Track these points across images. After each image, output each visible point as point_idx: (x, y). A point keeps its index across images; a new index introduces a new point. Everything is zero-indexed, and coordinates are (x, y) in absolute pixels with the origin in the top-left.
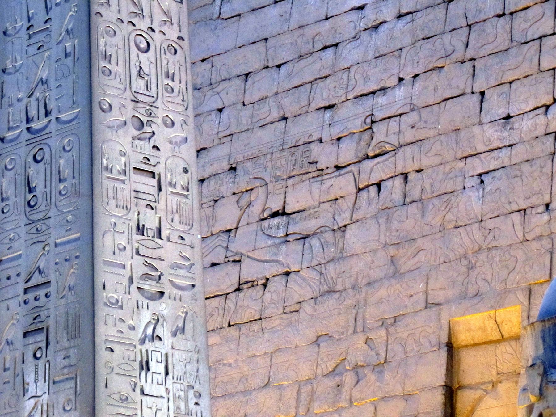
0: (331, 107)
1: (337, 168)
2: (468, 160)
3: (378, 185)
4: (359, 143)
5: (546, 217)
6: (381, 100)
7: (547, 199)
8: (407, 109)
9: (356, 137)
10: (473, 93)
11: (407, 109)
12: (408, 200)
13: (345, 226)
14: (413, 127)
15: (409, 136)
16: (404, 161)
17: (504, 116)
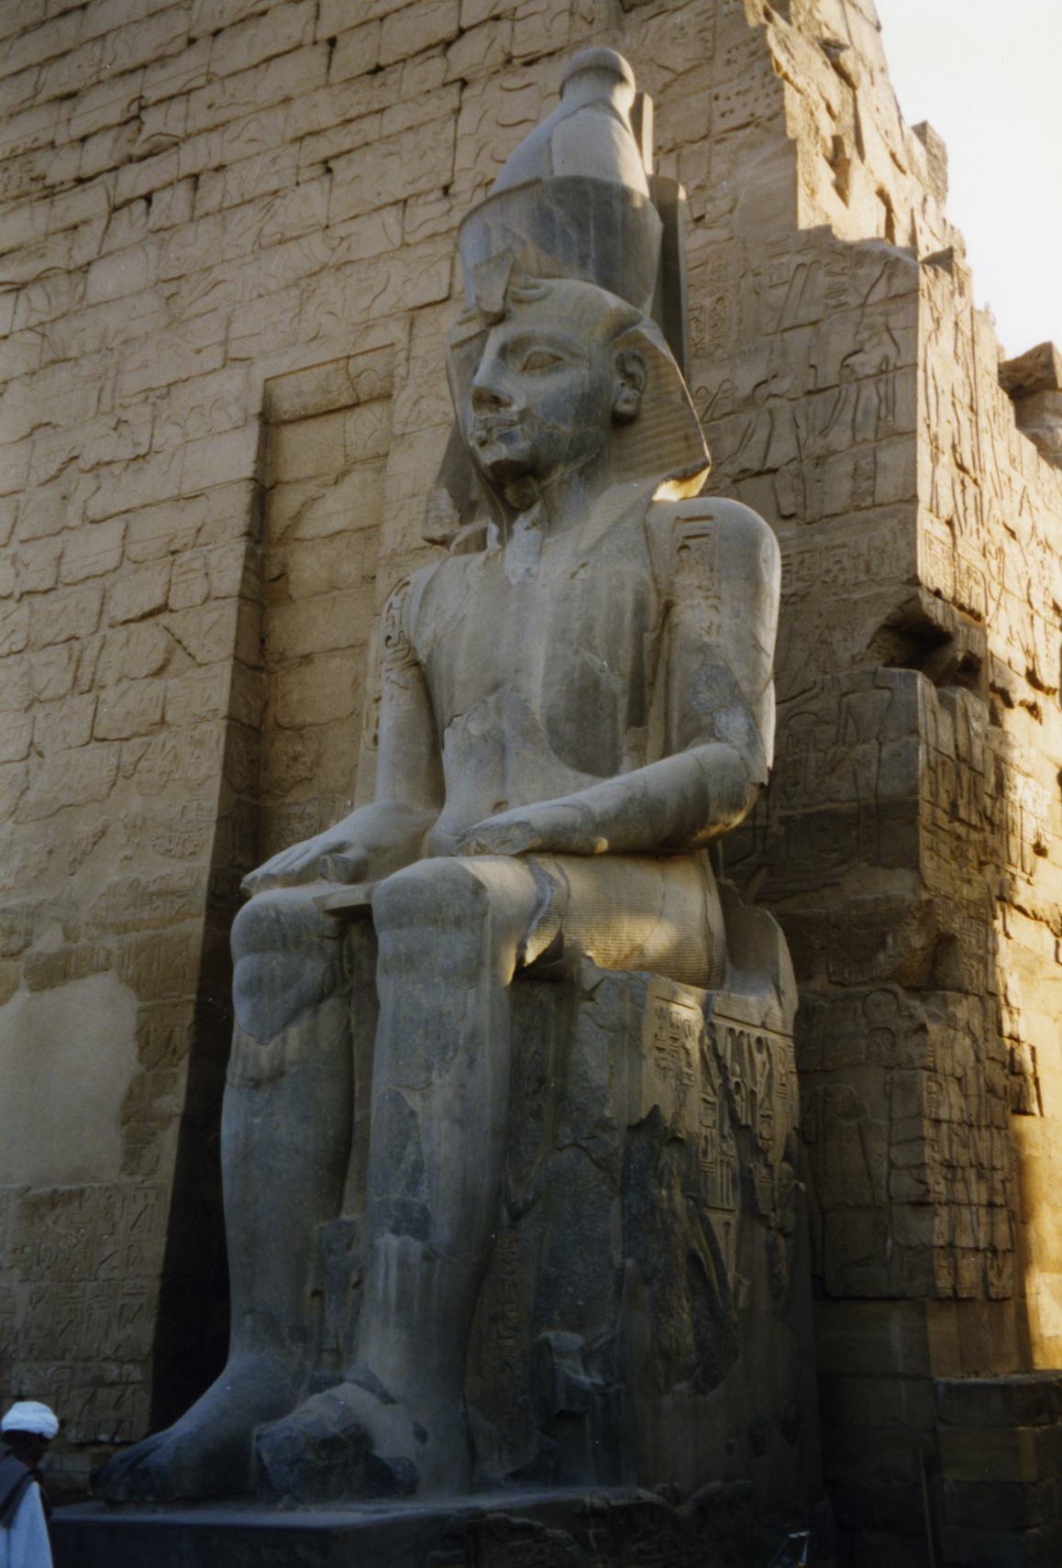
0: (71, 96)
1: (80, 181)
2: (308, 141)
3: (148, 199)
4: (116, 140)
5: (443, 206)
6: (157, 75)
7: (444, 180)
8: (202, 81)
9: (113, 133)
10: (315, 43)
11: (202, 81)
12: (198, 213)
13: (89, 264)
14: (210, 107)
15: (204, 120)
16: (192, 158)
17: (372, 67)
